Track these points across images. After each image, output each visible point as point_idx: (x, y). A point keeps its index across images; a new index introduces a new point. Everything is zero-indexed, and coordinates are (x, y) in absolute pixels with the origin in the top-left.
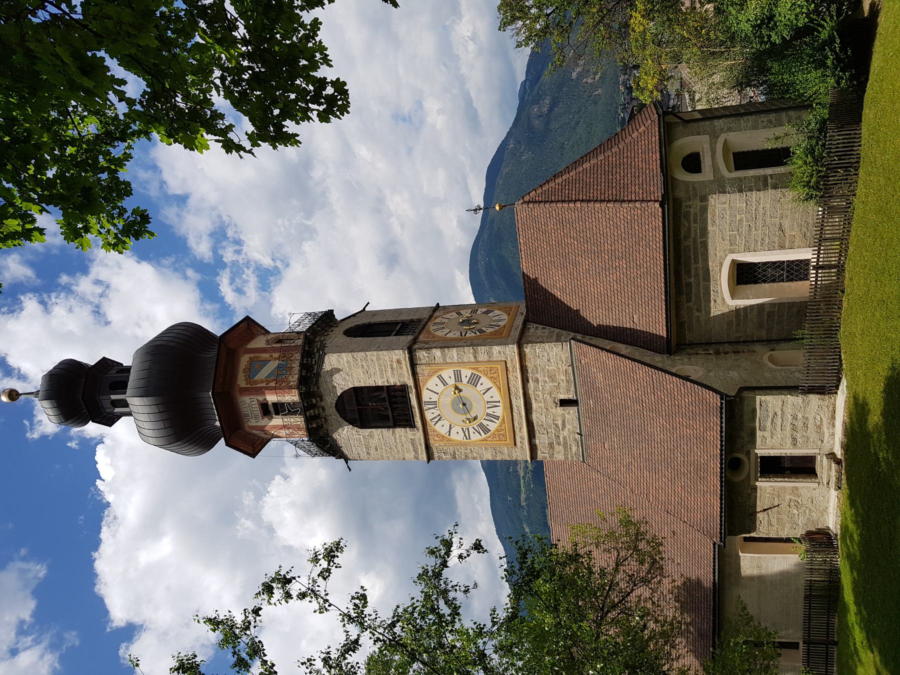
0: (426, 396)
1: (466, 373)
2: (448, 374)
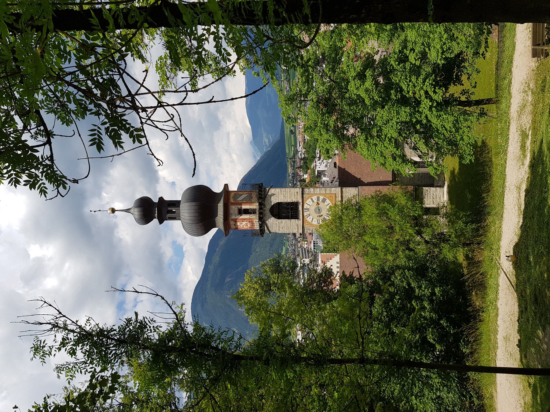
0: (306, 206)
1: (321, 198)
2: (315, 198)
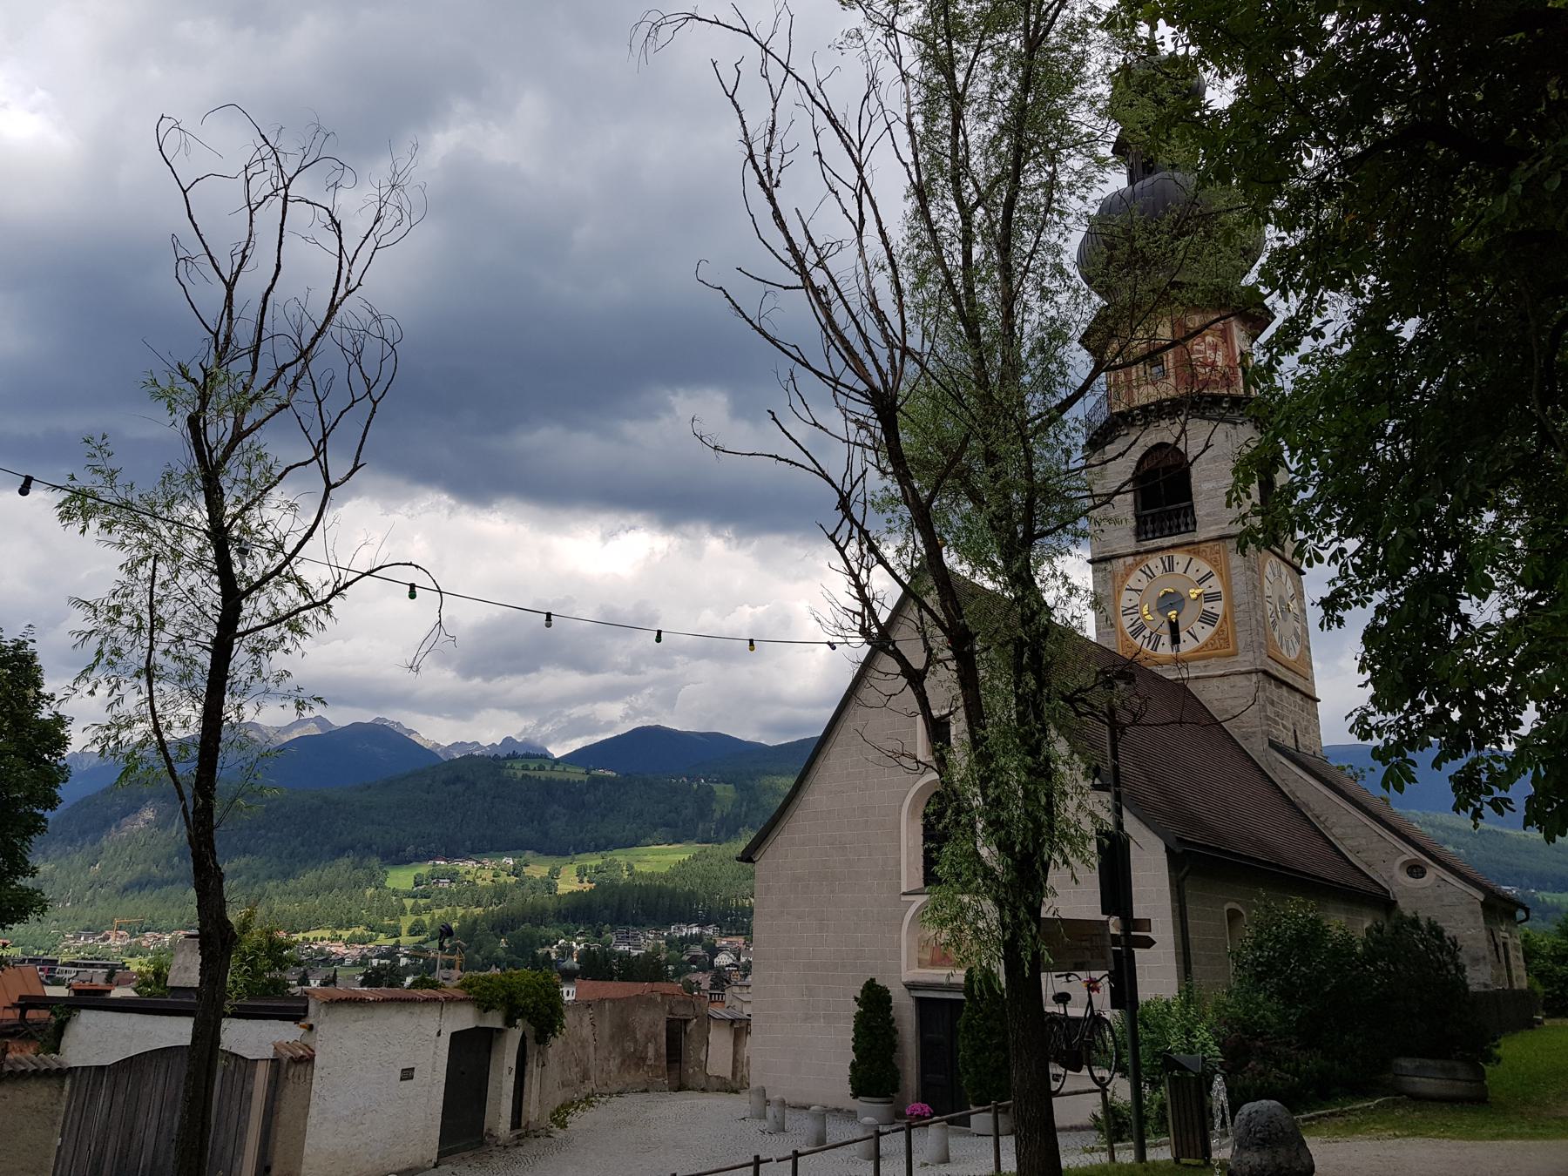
0: (1180, 558)
1: (1218, 608)
2: (1215, 585)
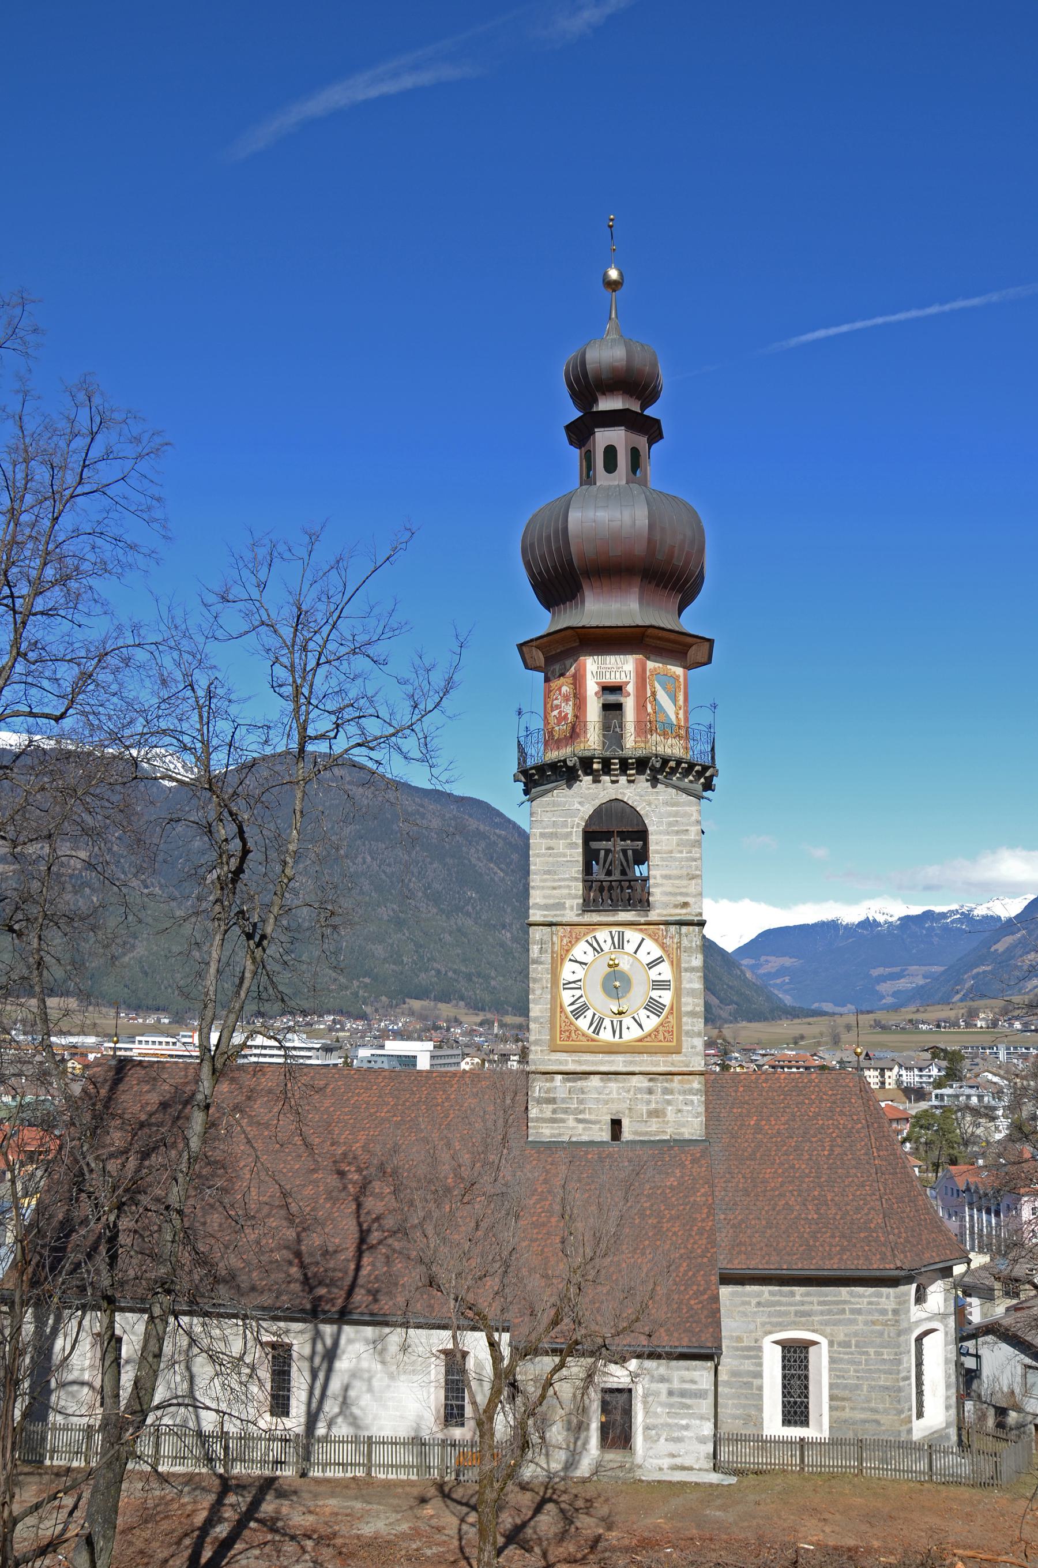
0: (632, 936)
1: (666, 997)
2: (665, 971)
